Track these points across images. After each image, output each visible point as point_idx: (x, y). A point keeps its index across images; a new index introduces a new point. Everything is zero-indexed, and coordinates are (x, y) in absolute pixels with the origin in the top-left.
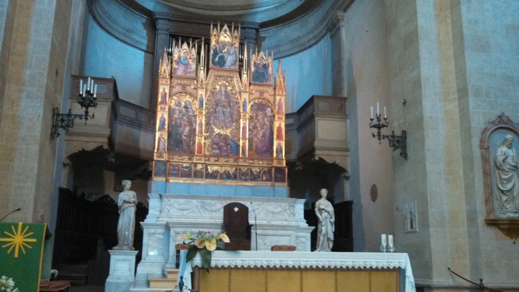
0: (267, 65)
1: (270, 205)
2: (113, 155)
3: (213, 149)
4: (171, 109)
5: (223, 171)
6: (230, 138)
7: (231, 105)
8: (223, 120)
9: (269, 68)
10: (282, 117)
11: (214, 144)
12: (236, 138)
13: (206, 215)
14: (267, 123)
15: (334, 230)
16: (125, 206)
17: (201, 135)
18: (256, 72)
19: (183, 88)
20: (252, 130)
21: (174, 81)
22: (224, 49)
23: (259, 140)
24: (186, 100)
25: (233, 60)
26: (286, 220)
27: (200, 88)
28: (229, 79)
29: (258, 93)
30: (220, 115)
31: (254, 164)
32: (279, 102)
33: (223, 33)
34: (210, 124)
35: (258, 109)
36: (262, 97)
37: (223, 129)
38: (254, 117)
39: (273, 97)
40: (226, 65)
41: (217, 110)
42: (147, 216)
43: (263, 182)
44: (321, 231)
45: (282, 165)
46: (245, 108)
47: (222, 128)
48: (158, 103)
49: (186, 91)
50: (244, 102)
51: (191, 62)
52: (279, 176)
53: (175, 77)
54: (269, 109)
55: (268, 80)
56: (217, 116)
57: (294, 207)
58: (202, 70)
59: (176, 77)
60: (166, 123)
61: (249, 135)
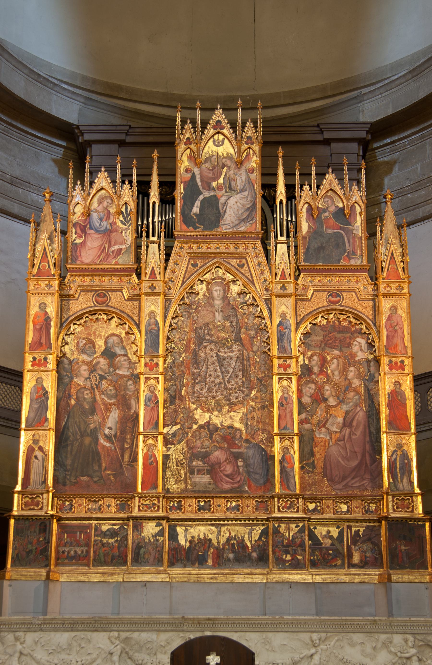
1: (352, 645)
3: (192, 472)
4: (66, 361)
8: (220, 383)
9: (355, 219)
10: (402, 362)
12: (262, 436)
14: (356, 382)
17: (154, 432)
19: (100, 299)
22: (216, 179)
23: (335, 437)
24: (110, 332)
27: (147, 295)
30: (211, 368)
32: (390, 318)
33: (212, 131)
34: (182, 399)
37: (220, 411)
38: (316, 369)
39: (371, 303)
40: (222, 222)
43: (353, 571)
45: (412, 511)
47: (219, 407)
48: (27, 348)
50: (280, 324)
51: (122, 222)
52: (403, 548)
53: (73, 271)
54: (362, 341)
55: (354, 253)
58: (153, 242)
60: (52, 403)
61: (301, 422)
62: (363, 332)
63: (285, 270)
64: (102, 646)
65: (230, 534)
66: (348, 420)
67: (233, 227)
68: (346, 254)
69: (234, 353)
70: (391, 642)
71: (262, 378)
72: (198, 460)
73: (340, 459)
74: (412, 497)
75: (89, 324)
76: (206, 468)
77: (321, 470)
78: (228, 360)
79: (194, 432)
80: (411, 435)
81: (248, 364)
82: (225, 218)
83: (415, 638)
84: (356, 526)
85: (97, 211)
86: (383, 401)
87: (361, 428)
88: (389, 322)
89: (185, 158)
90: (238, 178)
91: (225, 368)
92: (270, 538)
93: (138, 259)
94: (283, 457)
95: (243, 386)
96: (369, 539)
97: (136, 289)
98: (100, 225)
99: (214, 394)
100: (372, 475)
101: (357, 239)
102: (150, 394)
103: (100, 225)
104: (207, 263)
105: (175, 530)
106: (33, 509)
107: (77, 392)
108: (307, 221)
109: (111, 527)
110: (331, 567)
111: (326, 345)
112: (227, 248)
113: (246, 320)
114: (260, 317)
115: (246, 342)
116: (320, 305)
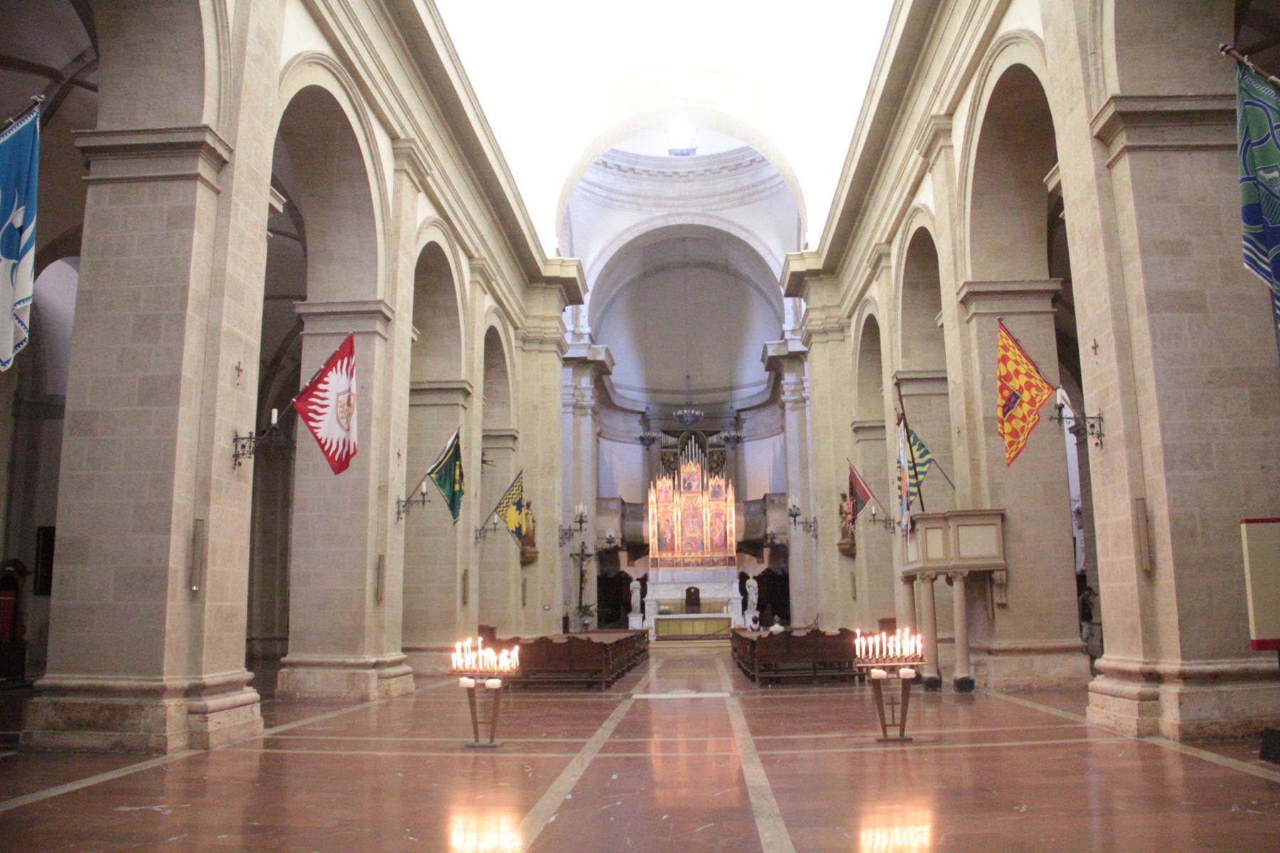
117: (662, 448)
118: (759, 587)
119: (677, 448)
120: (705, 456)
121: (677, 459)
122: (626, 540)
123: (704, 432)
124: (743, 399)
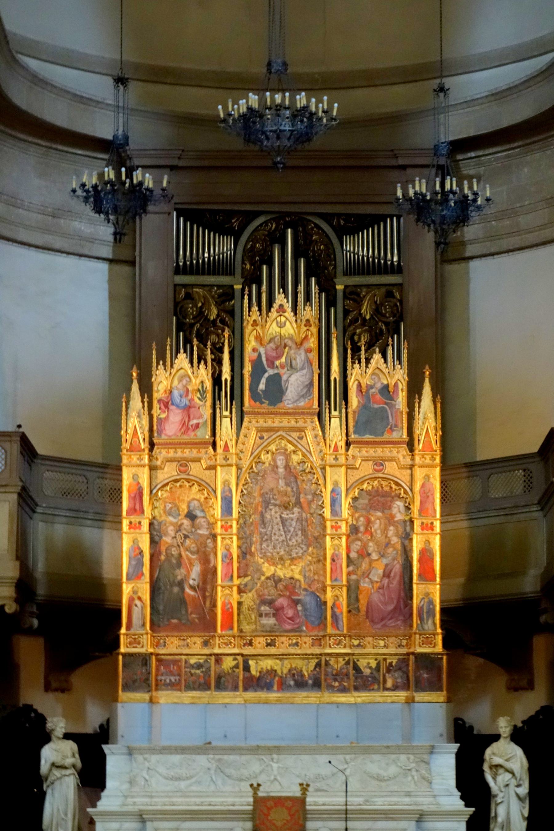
0: (391, 389)
2: (35, 609)
3: (261, 615)
4: (155, 522)
5: (285, 671)
6: (303, 587)
7: (302, 500)
8: (283, 541)
9: (398, 395)
10: (432, 523)
11: (263, 602)
13: (228, 788)
15: (526, 815)
16: (54, 775)
17: (230, 584)
18: (364, 407)
19: (182, 468)
20: (355, 562)
21: (160, 453)
22: (279, 357)
23: (376, 586)
24: (192, 497)
25: (303, 383)
26: (408, 794)
28: (295, 435)
29: (371, 463)
30: (276, 527)
31: (364, 647)
32: (423, 486)
34: (252, 554)
35: (372, 507)
36: (380, 475)
37: (283, 565)
38: (362, 529)
39: (409, 471)
40: (284, 398)
41: (268, 516)
42: (103, 794)
43: (386, 693)
44: (496, 816)
46: (337, 508)
49: (188, 474)
51: (199, 399)
52: (425, 676)
54: (400, 504)
55: (396, 426)
56: (268, 533)
57: (428, 763)
58: (226, 417)
59: (162, 444)
61: (349, 574)
62: (401, 496)
63: (338, 443)
64: (203, 764)
65: (291, 666)
66: (387, 572)
67: (294, 402)
68: (389, 427)
69: (295, 515)
70: (398, 760)
71: (318, 536)
72: (265, 605)
73: (380, 605)
74: (434, 635)
75: (174, 490)
76: (272, 612)
77: (364, 613)
78: (289, 521)
79: (262, 583)
80: (436, 585)
81: (306, 524)
82: (287, 394)
83: (415, 757)
84: (390, 659)
85: (177, 389)
86: (415, 556)
87: (398, 578)
88: (423, 489)
89: (252, 338)
90: (298, 357)
91: (287, 528)
92: (323, 669)
93: (214, 434)
94: (334, 604)
95: (302, 544)
96: (400, 669)
97: (212, 459)
98: (181, 401)
99: (278, 550)
100: (404, 617)
101: (399, 414)
102: (226, 551)
103: (181, 401)
104: (272, 436)
105: (248, 663)
106: (136, 647)
107: (166, 550)
108: (357, 397)
109: (197, 660)
110: (370, 690)
111: (370, 508)
112: (289, 422)
113: (305, 486)
114: (316, 483)
115: (305, 505)
116: (366, 473)
117: (178, 271)
118: (533, 771)
119: (229, 270)
120: (331, 303)
121: (231, 313)
122: (41, 591)
123: (327, 217)
124: (469, 103)
